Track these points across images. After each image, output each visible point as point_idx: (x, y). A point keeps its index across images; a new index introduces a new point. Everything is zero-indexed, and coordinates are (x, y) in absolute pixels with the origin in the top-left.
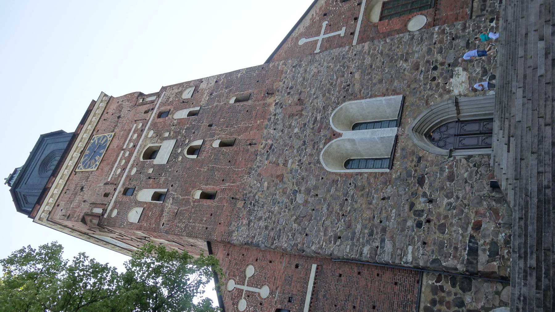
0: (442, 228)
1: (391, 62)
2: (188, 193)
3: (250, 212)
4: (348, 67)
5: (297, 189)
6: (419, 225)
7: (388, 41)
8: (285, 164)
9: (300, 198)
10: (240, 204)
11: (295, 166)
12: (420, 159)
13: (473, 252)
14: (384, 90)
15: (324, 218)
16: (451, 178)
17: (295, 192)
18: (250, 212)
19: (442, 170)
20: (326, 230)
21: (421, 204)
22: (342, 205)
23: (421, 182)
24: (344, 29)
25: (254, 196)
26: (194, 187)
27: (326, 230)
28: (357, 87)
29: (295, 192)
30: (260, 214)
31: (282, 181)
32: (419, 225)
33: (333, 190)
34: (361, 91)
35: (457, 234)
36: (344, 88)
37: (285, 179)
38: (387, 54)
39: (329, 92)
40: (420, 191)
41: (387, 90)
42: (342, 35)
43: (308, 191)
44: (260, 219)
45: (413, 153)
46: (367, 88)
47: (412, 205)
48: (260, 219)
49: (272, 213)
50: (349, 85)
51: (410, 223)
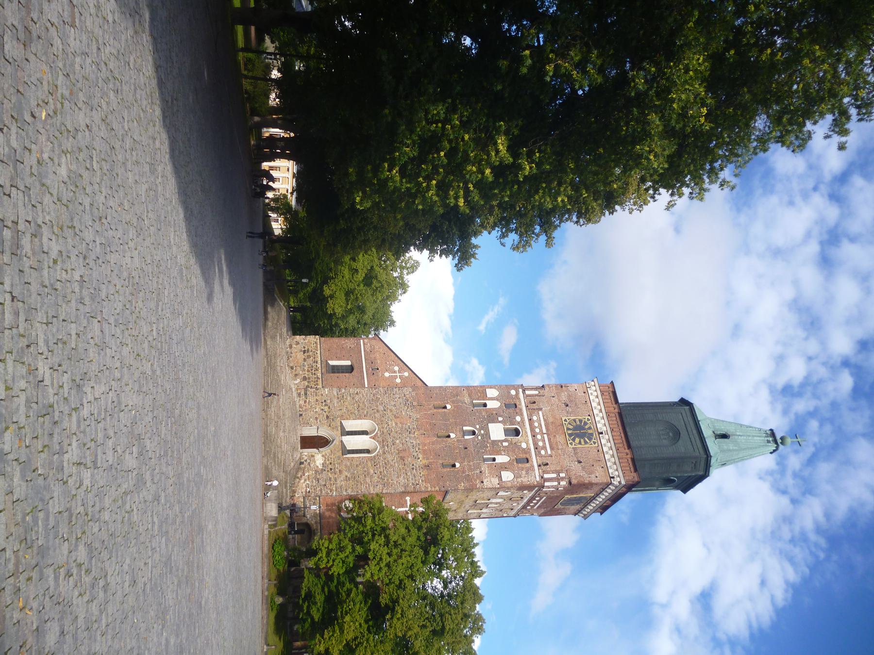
0: (317, 400)
2: (455, 407)
8: (396, 424)
9: (381, 408)
13: (306, 394)
16: (316, 418)
21: (326, 408)
23: (327, 417)
30: (401, 400)
35: (311, 399)
43: (378, 411)
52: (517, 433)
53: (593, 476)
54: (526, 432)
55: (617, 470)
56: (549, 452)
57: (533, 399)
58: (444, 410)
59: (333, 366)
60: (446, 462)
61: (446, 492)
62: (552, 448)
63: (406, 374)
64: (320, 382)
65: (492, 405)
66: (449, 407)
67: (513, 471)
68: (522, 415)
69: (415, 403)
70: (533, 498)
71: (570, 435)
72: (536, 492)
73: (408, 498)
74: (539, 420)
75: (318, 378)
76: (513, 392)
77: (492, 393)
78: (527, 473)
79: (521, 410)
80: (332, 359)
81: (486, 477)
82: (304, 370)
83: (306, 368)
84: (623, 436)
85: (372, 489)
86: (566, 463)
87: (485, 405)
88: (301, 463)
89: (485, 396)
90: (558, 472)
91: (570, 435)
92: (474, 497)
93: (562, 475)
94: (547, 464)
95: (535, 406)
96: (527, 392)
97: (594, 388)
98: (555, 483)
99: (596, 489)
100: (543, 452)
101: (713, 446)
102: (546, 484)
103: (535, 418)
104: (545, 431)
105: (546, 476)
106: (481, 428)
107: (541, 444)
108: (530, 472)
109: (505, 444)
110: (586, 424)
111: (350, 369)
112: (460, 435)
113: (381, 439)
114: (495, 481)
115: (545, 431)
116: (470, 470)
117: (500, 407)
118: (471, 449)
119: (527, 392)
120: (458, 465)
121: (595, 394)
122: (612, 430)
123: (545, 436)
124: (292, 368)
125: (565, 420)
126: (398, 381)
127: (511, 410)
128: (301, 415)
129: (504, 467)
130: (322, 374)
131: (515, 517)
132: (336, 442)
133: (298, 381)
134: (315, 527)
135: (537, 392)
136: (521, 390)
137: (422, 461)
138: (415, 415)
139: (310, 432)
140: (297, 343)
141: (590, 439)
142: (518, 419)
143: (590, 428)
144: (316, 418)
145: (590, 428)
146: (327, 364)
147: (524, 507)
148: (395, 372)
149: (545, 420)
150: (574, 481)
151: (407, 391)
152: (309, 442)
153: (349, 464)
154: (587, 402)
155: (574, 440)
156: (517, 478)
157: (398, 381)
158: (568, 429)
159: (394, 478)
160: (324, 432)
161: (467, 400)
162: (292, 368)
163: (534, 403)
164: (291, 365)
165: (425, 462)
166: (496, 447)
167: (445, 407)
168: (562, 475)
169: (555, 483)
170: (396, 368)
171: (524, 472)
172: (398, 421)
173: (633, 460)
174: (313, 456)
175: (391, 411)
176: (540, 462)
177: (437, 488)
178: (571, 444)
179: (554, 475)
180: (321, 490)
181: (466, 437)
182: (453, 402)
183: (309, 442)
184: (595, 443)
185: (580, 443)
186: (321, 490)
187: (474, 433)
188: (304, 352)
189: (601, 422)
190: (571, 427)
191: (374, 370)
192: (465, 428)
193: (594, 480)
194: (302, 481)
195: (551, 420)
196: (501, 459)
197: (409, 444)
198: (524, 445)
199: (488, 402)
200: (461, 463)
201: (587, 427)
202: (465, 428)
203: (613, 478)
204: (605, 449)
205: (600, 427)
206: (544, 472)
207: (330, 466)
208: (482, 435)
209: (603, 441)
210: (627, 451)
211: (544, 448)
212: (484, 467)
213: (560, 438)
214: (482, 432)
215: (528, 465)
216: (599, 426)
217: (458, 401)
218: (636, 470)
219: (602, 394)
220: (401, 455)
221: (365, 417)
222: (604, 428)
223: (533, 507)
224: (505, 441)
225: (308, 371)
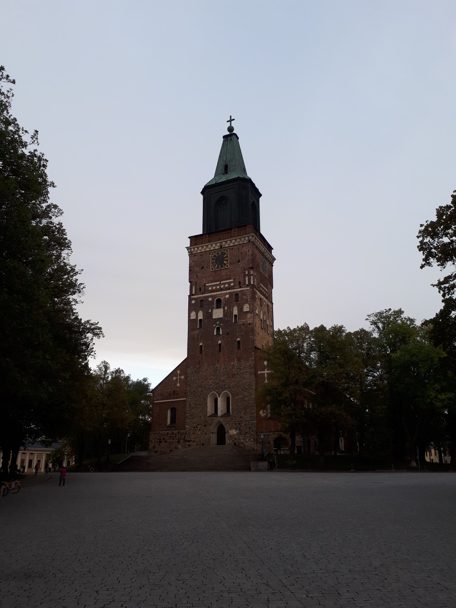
0: (194, 433)
4: (245, 392)
6: (194, 427)
8: (211, 379)
9: (200, 389)
10: (198, 366)
12: (211, 424)
13: (189, 441)
16: (206, 434)
17: (202, 386)
19: (208, 431)
20: (192, 401)
22: (198, 404)
23: (205, 426)
27: (192, 401)
31: (206, 380)
32: (194, 427)
39: (236, 387)
40: (202, 426)
45: (212, 422)
47: (199, 425)
51: (194, 425)
52: (219, 301)
55: (245, 238)
56: (232, 280)
57: (198, 289)
58: (203, 347)
59: (171, 422)
60: (236, 347)
61: (256, 348)
62: (230, 279)
63: (179, 372)
64: (181, 431)
65: (200, 316)
66: (201, 344)
67: (244, 304)
68: (208, 297)
69: (198, 366)
70: (261, 292)
71: (222, 267)
72: (257, 289)
73: (259, 372)
74: (212, 286)
75: (178, 433)
76: (193, 302)
77: (193, 316)
78: (245, 295)
79: (205, 297)
80: (167, 422)
82: (173, 442)
83: (172, 441)
84: (223, 233)
87: (201, 320)
88: (235, 444)
89: (195, 320)
90: (245, 275)
91: (222, 267)
92: (260, 329)
93: (247, 273)
94: (240, 282)
95: (203, 288)
96: (194, 293)
97: (192, 250)
98: (252, 278)
99: (256, 252)
100: (232, 284)
101: (232, 176)
102: (252, 283)
103: (210, 289)
104: (219, 283)
105: (247, 283)
107: (227, 286)
108: (244, 293)
109: (226, 308)
110: (215, 256)
111: (174, 410)
114: (249, 315)
115: (219, 283)
119: (194, 293)
120: (238, 339)
121: (196, 249)
122: (220, 239)
123: (222, 282)
124: (171, 451)
125: (212, 269)
126: (183, 377)
128: (203, 445)
129: (240, 310)
130: (176, 430)
131: (273, 304)
132: (221, 420)
133: (180, 446)
134: (276, 436)
136: (192, 297)
137: (235, 363)
139: (214, 438)
140: (154, 447)
141: (225, 254)
142: (210, 299)
144: (206, 434)
145: (218, 254)
146: (169, 426)
147: (267, 298)
148: (177, 379)
150: (251, 266)
152: (221, 439)
154: (202, 254)
155: (225, 264)
156: (247, 301)
157: (183, 377)
158: (218, 267)
160: (214, 429)
161: (197, 332)
162: (171, 451)
163: (200, 288)
164: (169, 451)
165: (236, 361)
166: (228, 314)
167: (201, 346)
168: (247, 273)
170: (174, 378)
171: (244, 297)
173: (238, 227)
174: (230, 436)
175: (202, 382)
176: (238, 287)
178: (227, 266)
179: (247, 278)
180: (252, 431)
181: (221, 334)
183: (221, 439)
184: (227, 251)
185: (227, 260)
186: (252, 431)
187: (218, 329)
188: (160, 442)
189: (215, 246)
190: (216, 266)
191: (175, 394)
192: (215, 334)
193: (251, 253)
194: (247, 444)
196: (235, 312)
198: (227, 296)
201: (217, 256)
202: (215, 334)
203: (249, 240)
204: (232, 245)
207: (237, 424)
208: (220, 323)
209: (227, 246)
210: (233, 231)
211: (229, 283)
212: (240, 322)
213: (224, 273)
214: (218, 323)
215: (240, 294)
216: (217, 248)
218: (245, 226)
219: (196, 244)
221: (206, 400)
222: (218, 244)
223: (266, 292)
224: (224, 308)
225: (174, 439)
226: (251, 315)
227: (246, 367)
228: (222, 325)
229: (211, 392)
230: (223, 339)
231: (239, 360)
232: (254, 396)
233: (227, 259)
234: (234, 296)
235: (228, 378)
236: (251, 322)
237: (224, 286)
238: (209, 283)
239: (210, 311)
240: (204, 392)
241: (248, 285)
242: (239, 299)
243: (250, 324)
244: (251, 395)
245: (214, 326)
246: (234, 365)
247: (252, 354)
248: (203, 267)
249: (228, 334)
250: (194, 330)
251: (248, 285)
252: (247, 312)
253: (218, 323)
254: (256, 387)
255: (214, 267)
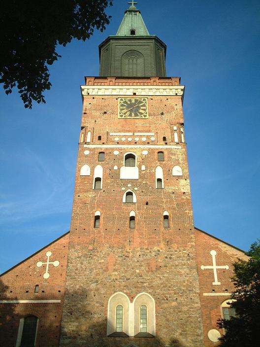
1: (181, 324)
2: (98, 207)
3: (85, 256)
5: (99, 282)
7: (199, 319)
8: (115, 270)
11: (113, 277)
14: (160, 324)
15: (82, 303)
17: (97, 282)
18: (85, 256)
24: (219, 283)
25: (95, 255)
26: (102, 209)
28: (166, 305)
29: (97, 282)
30: (85, 263)
31: (105, 271)
33: (97, 305)
34: (161, 308)
36: (165, 297)
37: (105, 273)
38: (188, 321)
41: (161, 326)
42: (214, 284)
43: (97, 290)
44: (82, 263)
46: (164, 313)
48: (82, 263)
49: (85, 271)
50: (167, 299)
52: (130, 157)
53: (175, 107)
54: (132, 149)
62: (149, 131)
65: (99, 172)
66: (98, 213)
68: (113, 149)
69: (91, 247)
71: (136, 115)
79: (107, 149)
81: (179, 189)
84: (137, 81)
85: (196, 305)
86: (164, 124)
87: (98, 179)
90: (173, 131)
91: (136, 115)
93: (175, 128)
94: (164, 139)
98: (182, 135)
100: (153, 139)
103: (117, 139)
104: (132, 134)
106: (125, 186)
107: (144, 139)
109: (143, 168)
110: (125, 102)
112: (132, 207)
113: (134, 290)
115: (132, 134)
116: (171, 202)
117: (104, 168)
118: (148, 198)
119: (88, 140)
120: (166, 213)
123: (135, 134)
125: (122, 116)
127: (107, 157)
129: (168, 172)
135: (89, 134)
136: (85, 146)
138: (106, 249)
141: (141, 102)
142: (116, 153)
143: (130, 101)
149: (120, 132)
150: (182, 121)
151: (73, 254)
153: (165, 330)
155: (141, 114)
156: (179, 163)
158: (130, 115)
159: (181, 279)
161: (91, 195)
163: (100, 138)
165: (162, 245)
167: (97, 218)
169: (182, 135)
171: (173, 157)
172: (111, 267)
175: (97, 274)
176: (163, 143)
177: (192, 236)
178: (145, 116)
179: (176, 134)
181: (135, 200)
182: (93, 208)
195: (119, 127)
196: (159, 173)
197: (141, 259)
198: (145, 153)
199: (95, 176)
200: (164, 210)
202: (124, 201)
205: (130, 92)
206: (173, 141)
208: (133, 186)
211: (148, 137)
212: (170, 189)
213: (139, 123)
214: (129, 185)
215: (166, 153)
217: (92, 201)
220: (154, 269)
226: (185, 182)
227: (180, 257)
228: (136, 189)
229: (115, 292)
230: (138, 209)
231: (168, 243)
232: (199, 305)
233: (145, 108)
234: (156, 154)
235: (148, 272)
236: (185, 191)
237: (140, 140)
238: (115, 132)
239: (116, 168)
240: (103, 291)
241: (178, 143)
242: (165, 159)
243: (184, 193)
244: (194, 302)
245: (123, 189)
246: (159, 251)
247: (192, 238)
248: (105, 113)
249: (147, 204)
250: (87, 191)
251: (178, 143)
252: (179, 177)
253: (129, 185)
254: (200, 289)
255: (125, 114)
